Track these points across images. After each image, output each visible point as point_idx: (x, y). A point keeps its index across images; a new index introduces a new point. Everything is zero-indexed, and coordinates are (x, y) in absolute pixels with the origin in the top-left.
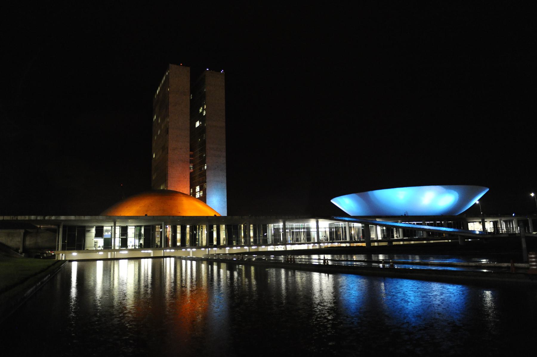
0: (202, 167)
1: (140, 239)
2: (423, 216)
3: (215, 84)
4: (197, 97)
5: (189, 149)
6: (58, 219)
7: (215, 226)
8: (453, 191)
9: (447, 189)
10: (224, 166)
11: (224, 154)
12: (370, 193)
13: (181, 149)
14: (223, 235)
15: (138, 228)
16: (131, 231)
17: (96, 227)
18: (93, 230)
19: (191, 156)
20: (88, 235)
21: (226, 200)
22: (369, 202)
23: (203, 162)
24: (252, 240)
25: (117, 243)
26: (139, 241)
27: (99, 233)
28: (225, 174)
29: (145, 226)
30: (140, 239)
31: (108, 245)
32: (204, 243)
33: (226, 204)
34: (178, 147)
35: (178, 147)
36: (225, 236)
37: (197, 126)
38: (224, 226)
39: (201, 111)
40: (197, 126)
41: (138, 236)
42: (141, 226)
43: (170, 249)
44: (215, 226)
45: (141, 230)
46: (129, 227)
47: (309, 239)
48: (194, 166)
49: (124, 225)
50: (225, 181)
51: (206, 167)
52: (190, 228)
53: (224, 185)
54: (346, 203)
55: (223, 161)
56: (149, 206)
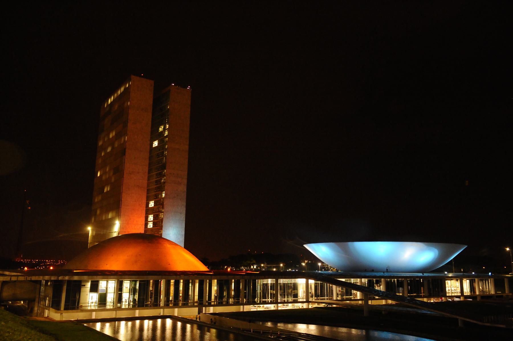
0: (159, 194)
1: (134, 294)
3: (180, 100)
4: (159, 115)
6: (71, 279)
10: (184, 195)
11: (185, 181)
12: (350, 244)
13: (138, 173)
15: (133, 283)
17: (92, 282)
18: (89, 285)
20: (83, 289)
21: (183, 233)
23: (160, 189)
25: (111, 298)
27: (94, 288)
28: (185, 204)
29: (140, 281)
30: (134, 294)
31: (103, 300)
34: (136, 171)
35: (136, 171)
37: (154, 146)
38: (216, 281)
39: (161, 129)
40: (154, 146)
41: (133, 291)
42: (136, 281)
45: (135, 285)
50: (184, 212)
51: (164, 195)
52: (183, 282)
53: (183, 217)
54: (322, 251)
55: (183, 188)
56: (137, 256)
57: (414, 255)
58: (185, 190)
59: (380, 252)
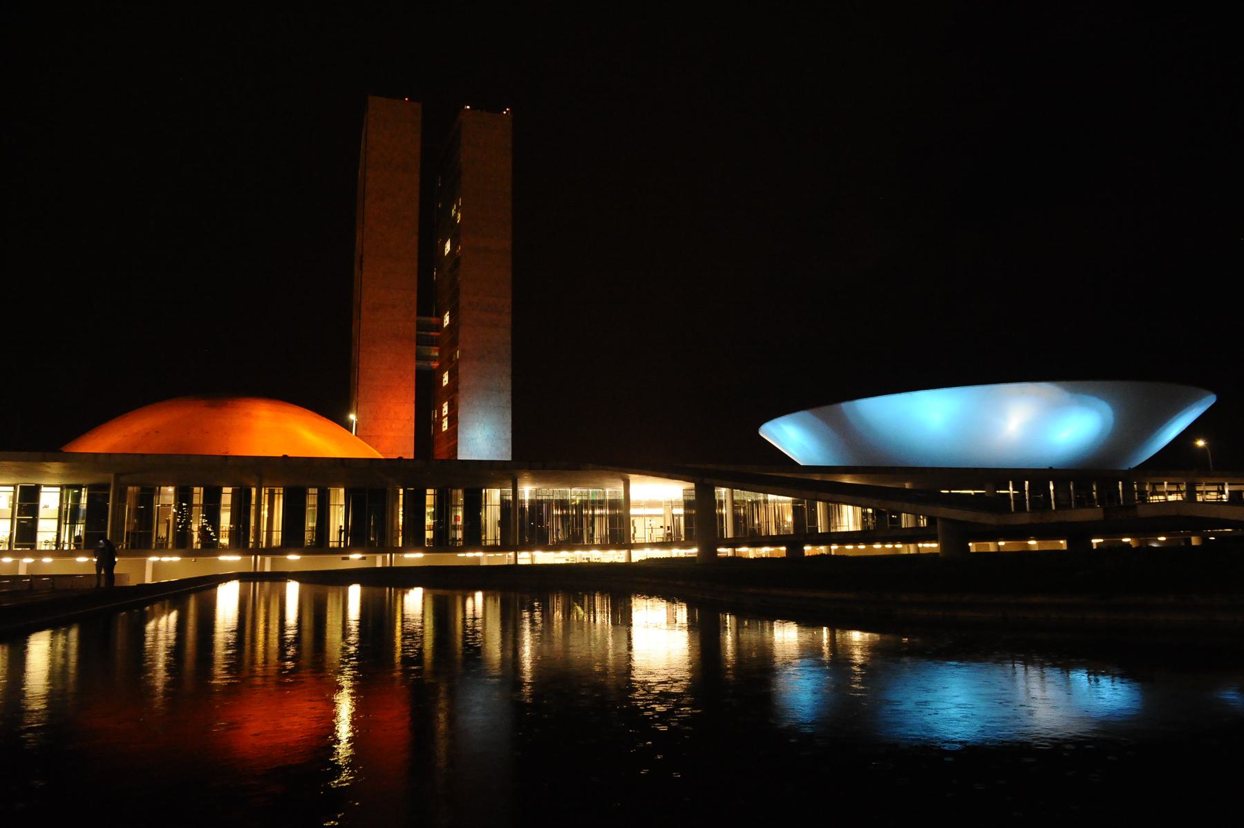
2: (976, 470)
5: (414, 308)
7: (313, 491)
8: (1093, 400)
9: (1074, 391)
11: (507, 319)
12: (845, 406)
14: (338, 519)
16: (50, 500)
19: (420, 326)
21: (509, 435)
22: (844, 432)
24: (429, 535)
26: (72, 530)
28: (509, 370)
29: (92, 488)
30: (73, 522)
32: (277, 538)
33: (510, 445)
36: (342, 523)
41: (69, 515)
42: (79, 487)
43: (170, 554)
44: (313, 491)
45: (77, 498)
46: (43, 489)
47: (619, 536)
48: (440, 351)
49: (31, 482)
50: (509, 387)
53: (506, 397)
54: (792, 437)
55: (503, 336)
56: (147, 434)
57: (1038, 424)
58: (509, 338)
59: (930, 420)
